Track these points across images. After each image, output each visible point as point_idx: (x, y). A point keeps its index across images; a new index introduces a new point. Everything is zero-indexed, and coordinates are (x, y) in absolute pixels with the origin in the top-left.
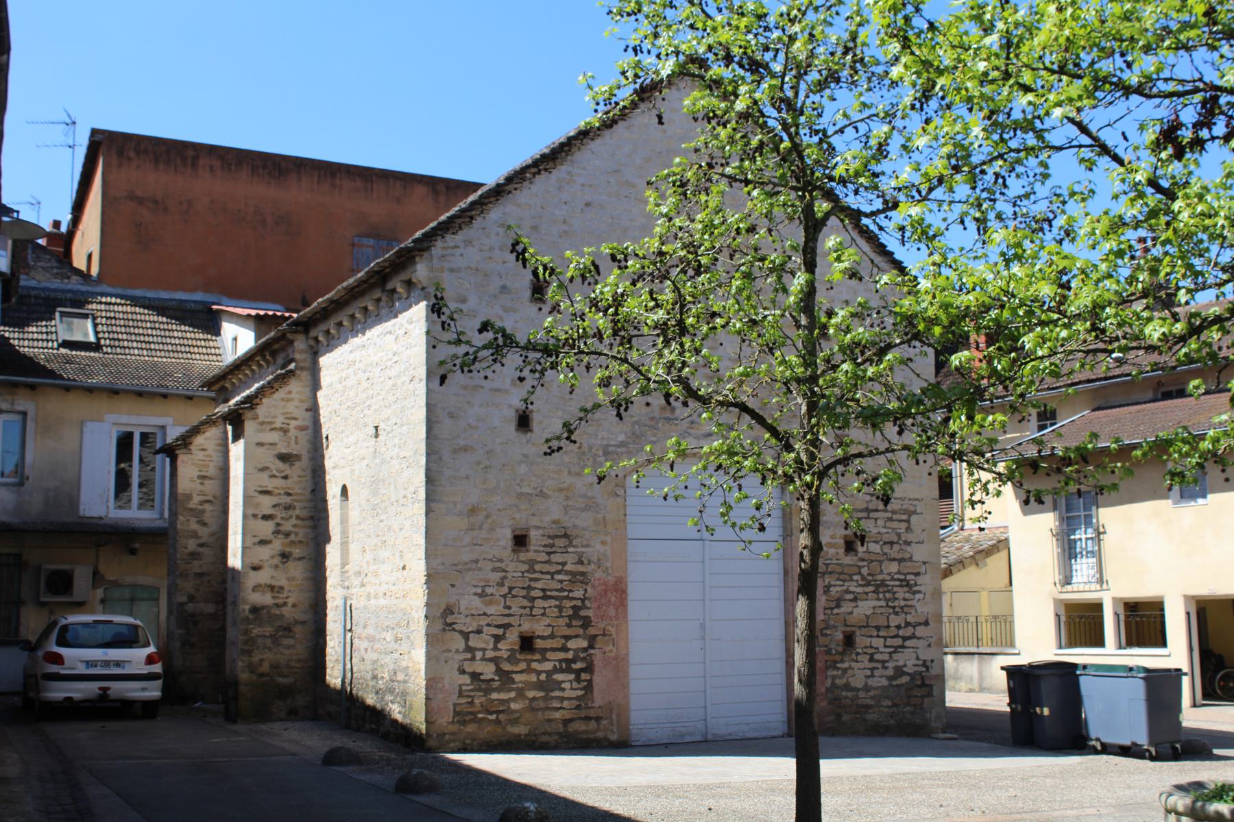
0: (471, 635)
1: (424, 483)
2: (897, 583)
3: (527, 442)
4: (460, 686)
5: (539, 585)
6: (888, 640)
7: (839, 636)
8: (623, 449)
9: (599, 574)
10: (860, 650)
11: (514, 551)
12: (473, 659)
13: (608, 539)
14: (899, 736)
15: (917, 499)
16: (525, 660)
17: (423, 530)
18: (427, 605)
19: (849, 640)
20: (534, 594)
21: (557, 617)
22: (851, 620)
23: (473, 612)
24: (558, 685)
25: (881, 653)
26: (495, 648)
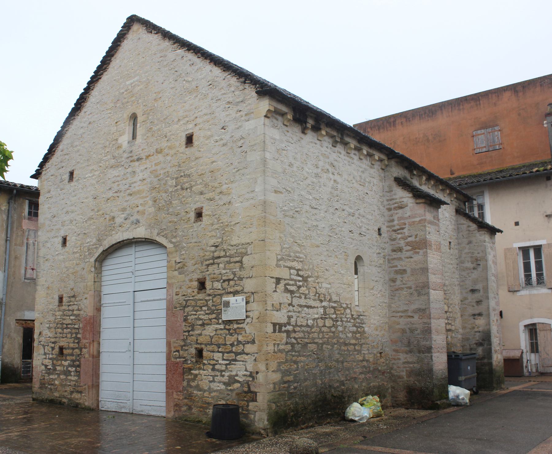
6: (225, 354)
7: (193, 351)
10: (205, 362)
15: (248, 243)
19: (200, 353)
22: (201, 339)
25: (220, 364)
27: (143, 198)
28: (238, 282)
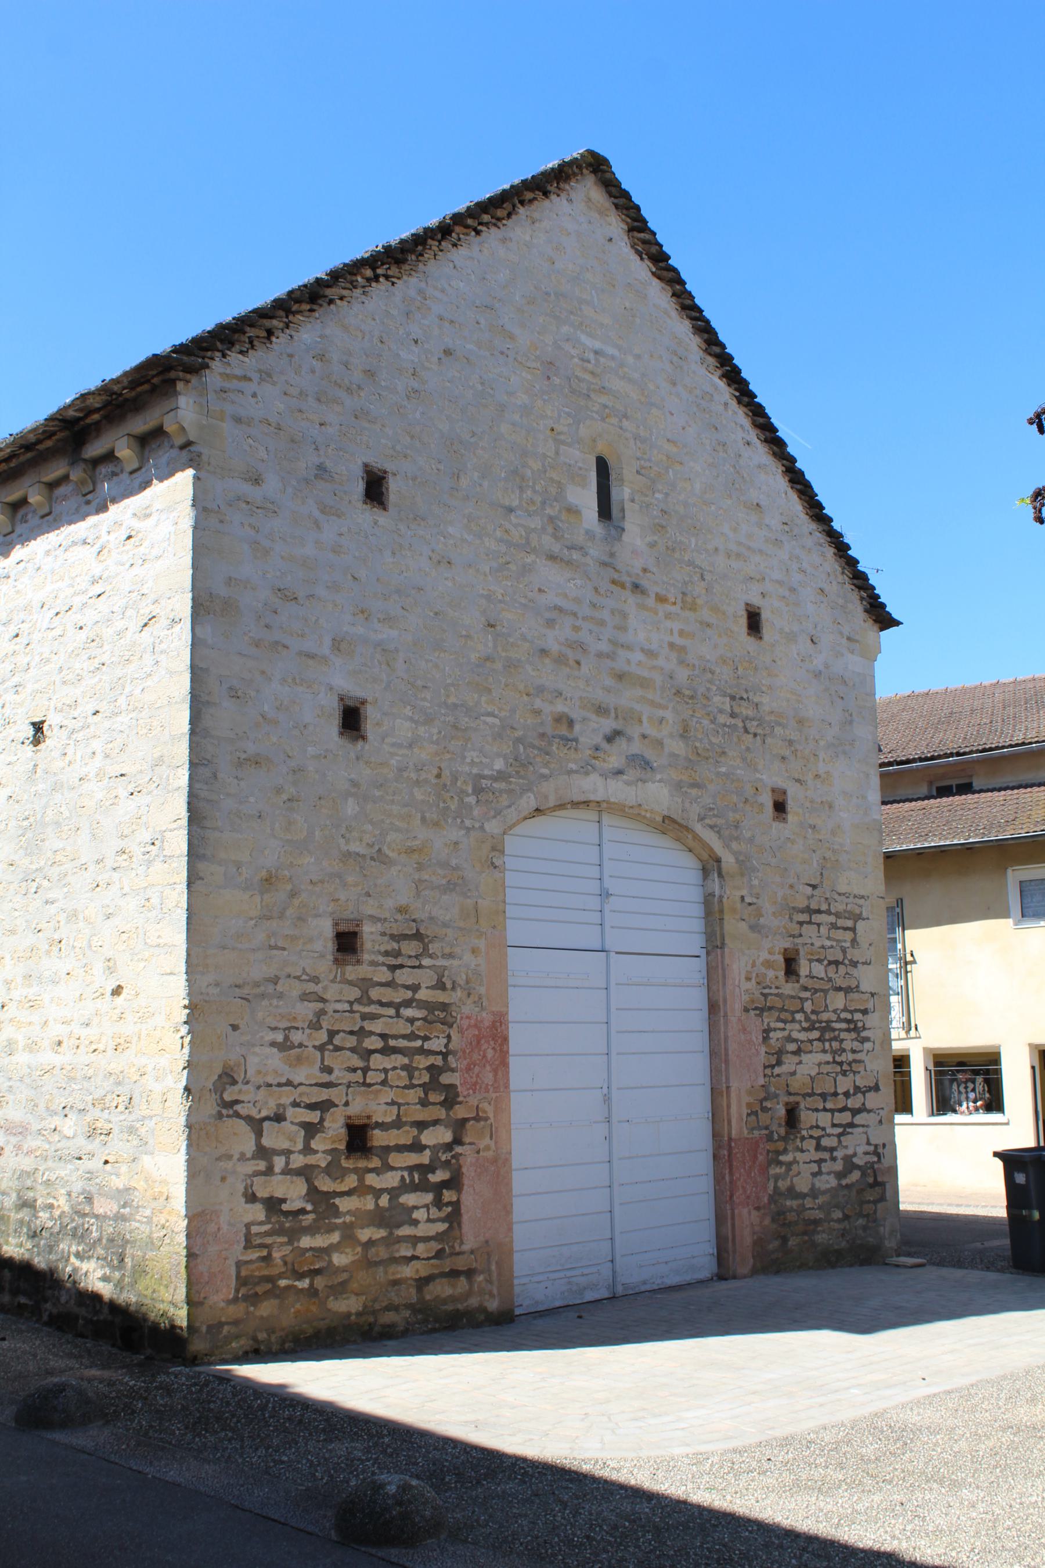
0: (266, 1124)
1: (185, 822)
2: (844, 1026)
3: (358, 758)
4: (248, 1226)
5: (377, 1027)
7: (781, 1111)
8: (503, 785)
9: (466, 1010)
10: (804, 1133)
11: (336, 961)
12: (269, 1171)
13: (482, 944)
14: (851, 1265)
15: (863, 897)
16: (356, 1170)
17: (182, 916)
18: (189, 1065)
20: (373, 1043)
21: (405, 1087)
22: (796, 1085)
23: (270, 1079)
24: (407, 1217)
25: (829, 1135)
26: (307, 1150)
27: (653, 704)
28: (850, 969)
